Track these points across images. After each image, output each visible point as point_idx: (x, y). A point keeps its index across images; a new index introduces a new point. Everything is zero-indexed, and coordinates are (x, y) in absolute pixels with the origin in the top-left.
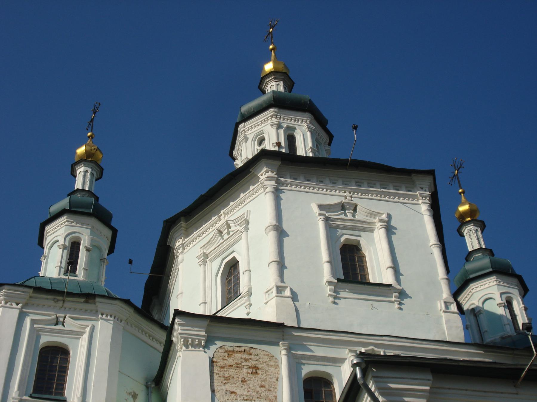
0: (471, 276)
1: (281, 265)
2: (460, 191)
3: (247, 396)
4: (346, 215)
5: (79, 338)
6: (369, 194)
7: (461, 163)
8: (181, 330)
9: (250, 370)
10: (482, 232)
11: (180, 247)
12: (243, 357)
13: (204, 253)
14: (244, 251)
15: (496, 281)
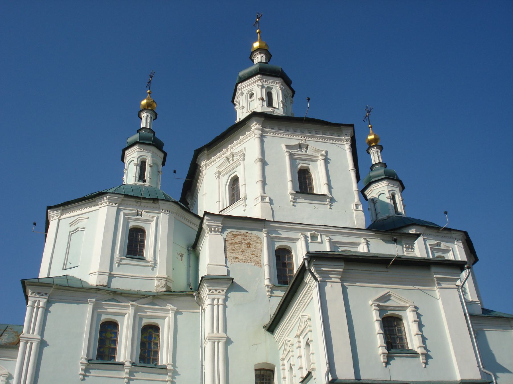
0: (373, 180)
1: (264, 183)
2: (370, 126)
3: (244, 260)
4: (302, 151)
5: (150, 224)
6: (315, 138)
7: (370, 109)
8: (208, 222)
9: (246, 246)
10: (381, 152)
11: (204, 166)
12: (242, 238)
13: (218, 171)
14: (242, 173)
15: (387, 183)
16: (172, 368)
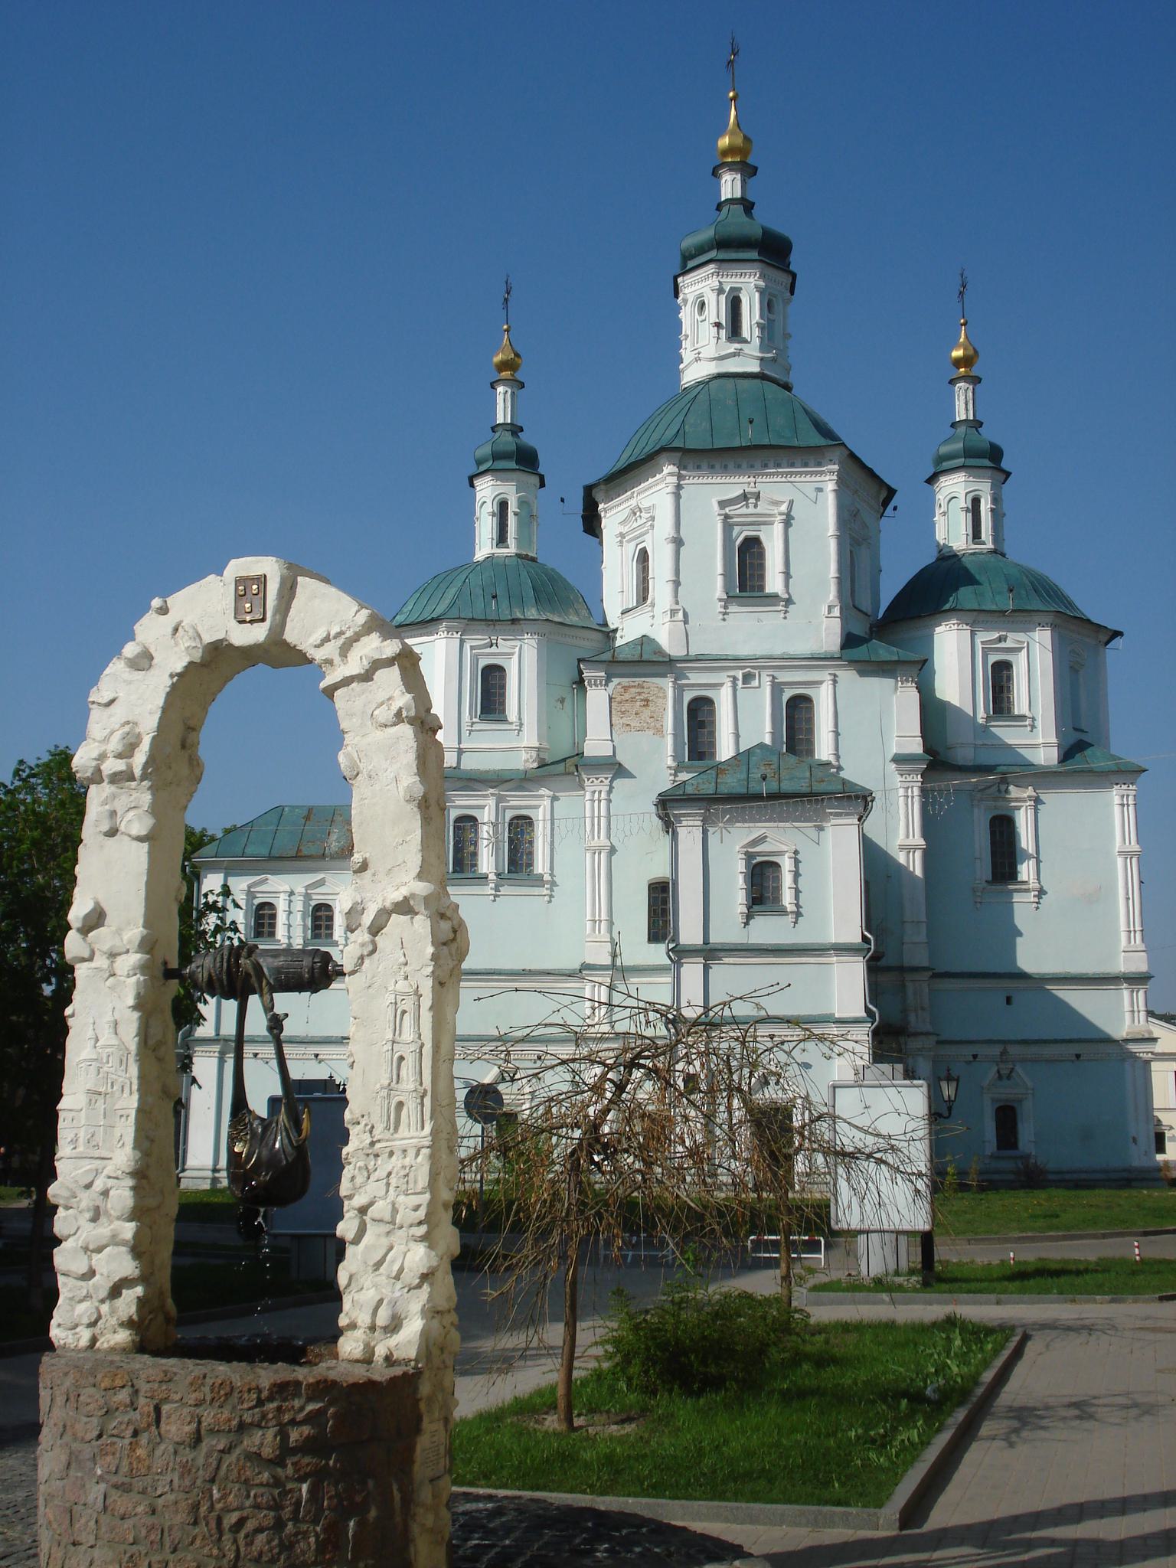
1: (677, 583)
2: (962, 321)
4: (747, 507)
13: (621, 533)
14: (651, 547)
16: (549, 878)
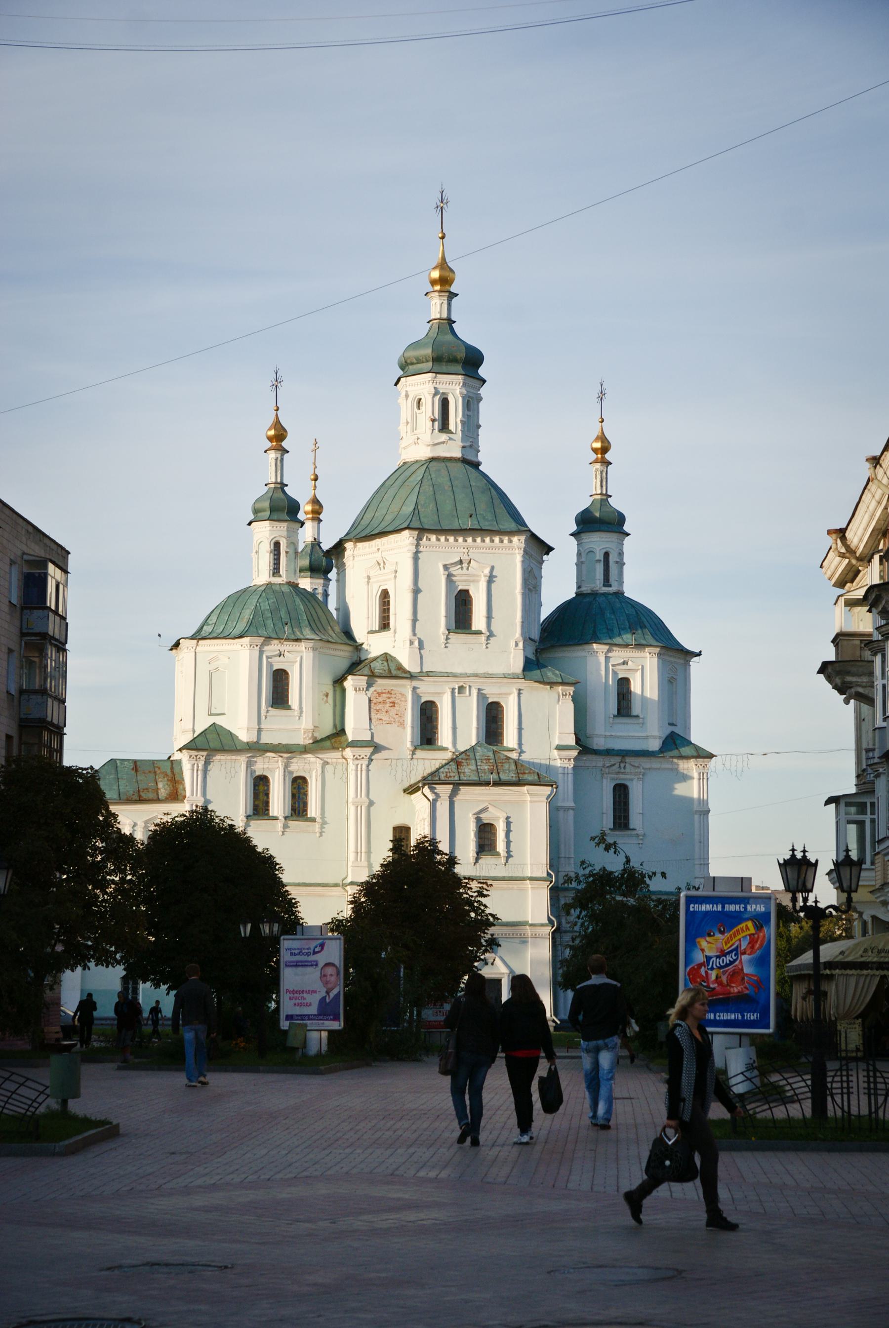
9: (391, 704)
